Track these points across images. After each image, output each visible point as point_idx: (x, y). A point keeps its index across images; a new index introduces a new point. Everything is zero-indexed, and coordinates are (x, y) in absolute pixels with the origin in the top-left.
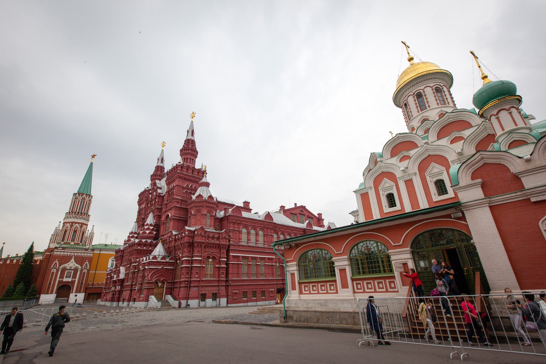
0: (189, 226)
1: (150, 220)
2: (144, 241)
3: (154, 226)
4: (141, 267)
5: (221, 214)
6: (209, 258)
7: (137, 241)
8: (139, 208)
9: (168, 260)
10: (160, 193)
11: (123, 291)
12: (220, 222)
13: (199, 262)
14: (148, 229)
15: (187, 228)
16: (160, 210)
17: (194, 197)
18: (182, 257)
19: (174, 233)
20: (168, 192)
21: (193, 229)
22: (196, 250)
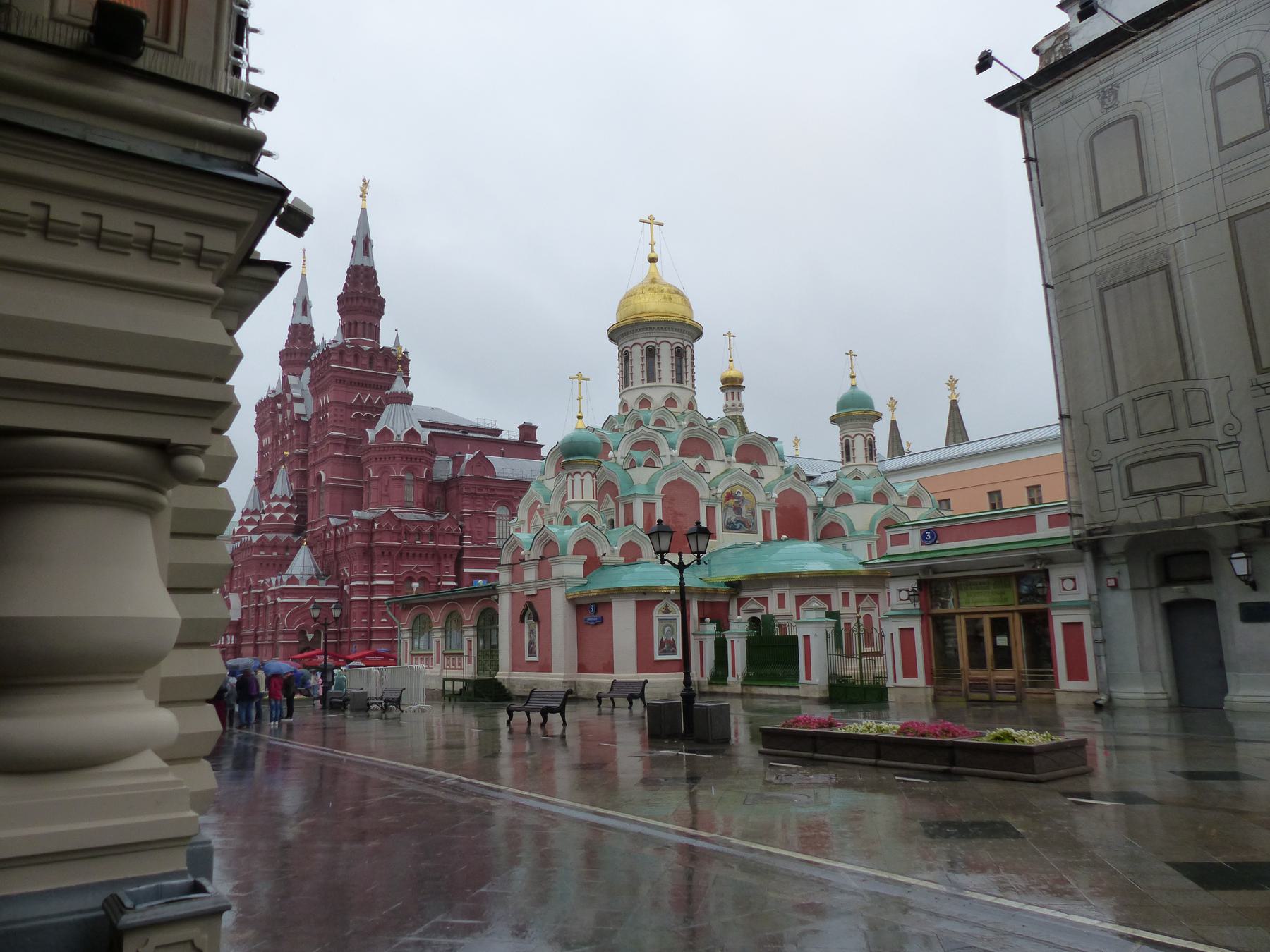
0: (360, 509)
1: (282, 486)
2: (270, 537)
3: (292, 501)
4: (269, 598)
5: (443, 469)
6: (411, 580)
7: (255, 538)
8: (260, 442)
9: (322, 584)
10: (298, 415)
11: (241, 646)
12: (440, 494)
13: (389, 589)
14: (278, 509)
15: (355, 513)
16: (304, 458)
17: (371, 434)
18: (352, 579)
19: (333, 522)
20: (317, 414)
21: (367, 515)
22: (379, 563)
